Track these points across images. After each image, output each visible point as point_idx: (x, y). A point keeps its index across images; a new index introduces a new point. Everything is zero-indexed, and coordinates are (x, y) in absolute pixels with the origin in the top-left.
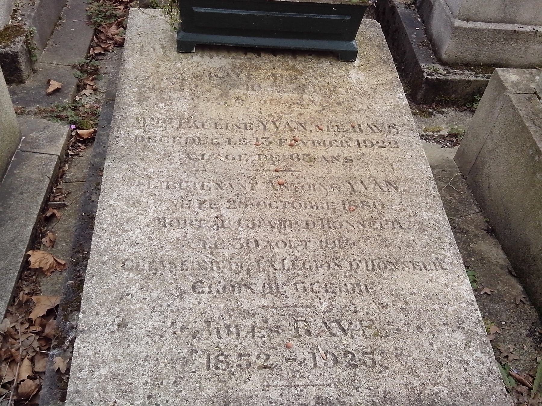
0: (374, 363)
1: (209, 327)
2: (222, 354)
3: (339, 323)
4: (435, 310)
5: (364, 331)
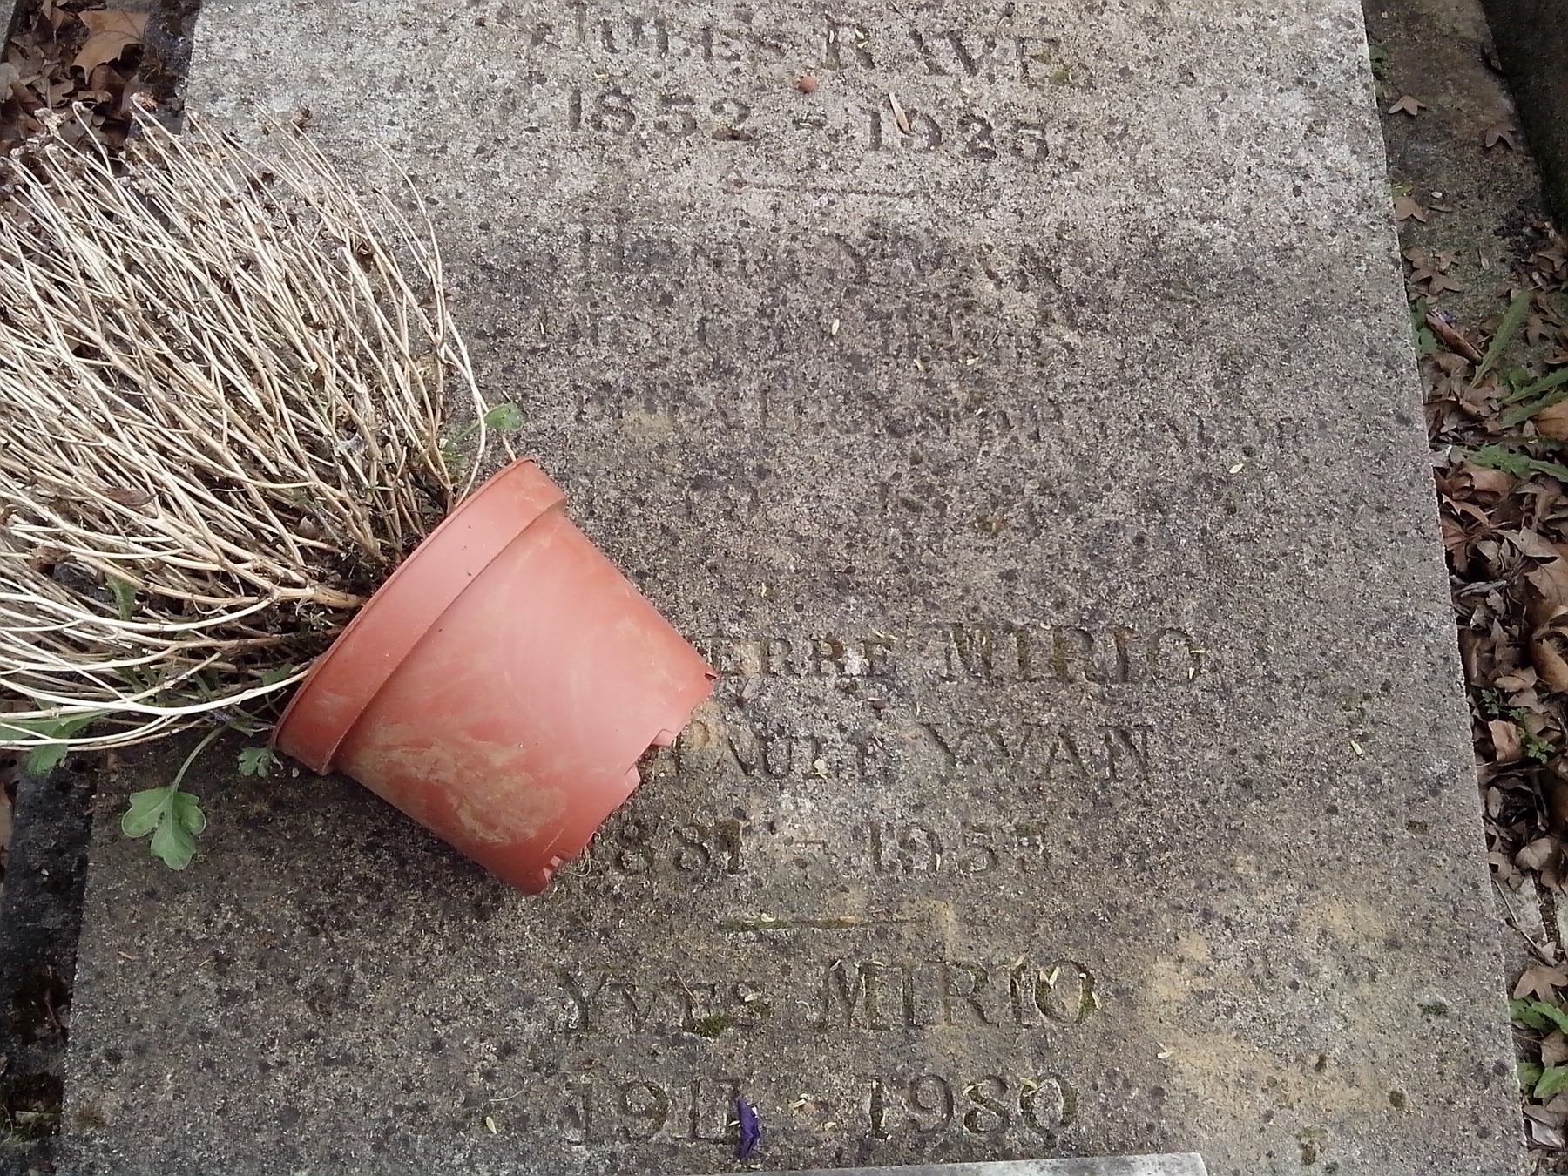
0: (1044, 150)
1: (581, 18)
2: (617, 92)
3: (957, 40)
4: (1240, 28)
5: (1025, 68)
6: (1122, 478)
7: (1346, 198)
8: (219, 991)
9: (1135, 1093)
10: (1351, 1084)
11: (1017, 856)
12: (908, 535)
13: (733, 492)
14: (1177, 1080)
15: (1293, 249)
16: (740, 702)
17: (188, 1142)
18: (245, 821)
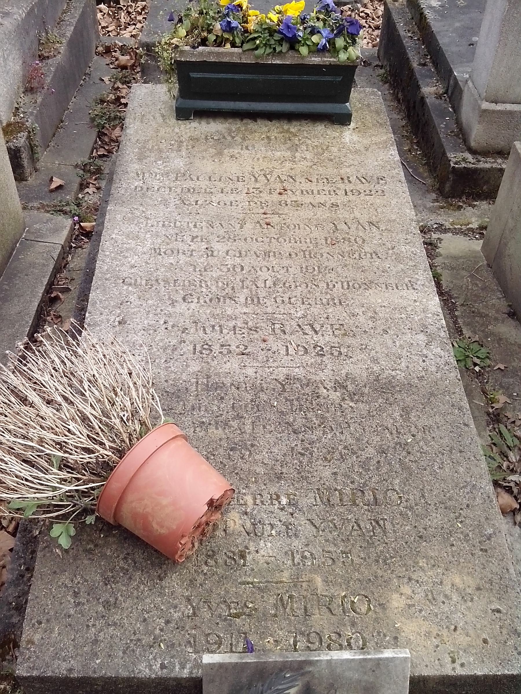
0: (340, 353)
1: (196, 326)
2: (207, 344)
3: (312, 326)
4: (402, 318)
5: (334, 332)
6: (371, 444)
7: (440, 362)
8: (74, 602)
9: (388, 638)
10: (467, 636)
11: (342, 560)
12: (301, 462)
13: (243, 451)
14: (403, 634)
15: (424, 377)
16: (246, 513)
17: (62, 649)
18: (86, 551)
